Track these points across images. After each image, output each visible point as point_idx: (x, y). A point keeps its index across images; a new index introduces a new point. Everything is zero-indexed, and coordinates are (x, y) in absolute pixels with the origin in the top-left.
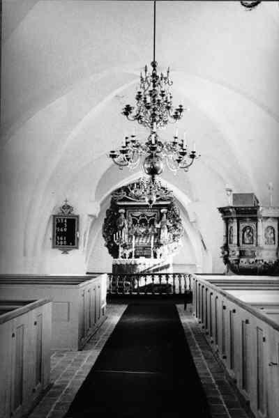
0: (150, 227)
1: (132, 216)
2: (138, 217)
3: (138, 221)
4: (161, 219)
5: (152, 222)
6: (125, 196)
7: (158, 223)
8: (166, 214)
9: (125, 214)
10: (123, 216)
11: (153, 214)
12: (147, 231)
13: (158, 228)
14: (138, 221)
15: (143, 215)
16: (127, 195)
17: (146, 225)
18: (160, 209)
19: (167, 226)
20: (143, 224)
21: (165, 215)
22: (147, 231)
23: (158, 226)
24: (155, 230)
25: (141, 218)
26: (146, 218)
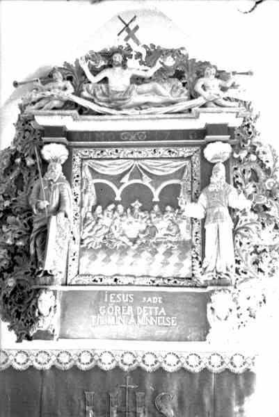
0: (163, 211)
1: (95, 174)
2: (117, 179)
3: (118, 193)
4: (206, 182)
5: (170, 199)
6: (69, 94)
7: (195, 199)
8: (226, 163)
9: (67, 167)
10: (57, 171)
11: (172, 167)
13: (193, 220)
14: (118, 193)
15: (137, 173)
16: (78, 93)
17: (147, 208)
18: (203, 146)
19: (232, 210)
20: (137, 205)
21: (222, 167)
22: (151, 231)
23: (194, 210)
24: (183, 226)
25: (126, 181)
26: (146, 181)
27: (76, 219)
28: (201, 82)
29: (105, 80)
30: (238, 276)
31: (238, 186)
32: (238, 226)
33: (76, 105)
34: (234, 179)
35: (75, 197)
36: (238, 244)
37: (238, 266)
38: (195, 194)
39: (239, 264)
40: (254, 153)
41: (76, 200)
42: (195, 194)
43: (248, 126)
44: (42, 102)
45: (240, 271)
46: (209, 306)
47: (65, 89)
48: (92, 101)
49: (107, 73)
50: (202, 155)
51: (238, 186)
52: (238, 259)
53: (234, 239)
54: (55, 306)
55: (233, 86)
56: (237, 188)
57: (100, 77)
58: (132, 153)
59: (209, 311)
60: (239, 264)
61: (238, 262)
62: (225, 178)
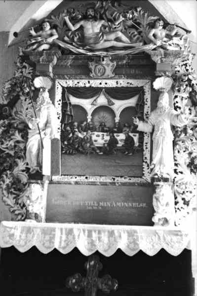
12: (113, 142)
28: (153, 31)
29: (82, 28)
30: (176, 175)
31: (178, 109)
32: (177, 139)
33: (60, 47)
34: (175, 104)
35: (58, 116)
36: (176, 152)
37: (176, 168)
38: (146, 115)
39: (177, 166)
40: (190, 86)
41: (59, 118)
42: (146, 115)
43: (186, 65)
44: (35, 47)
45: (178, 171)
46: (154, 195)
47: (51, 35)
48: (71, 44)
49: (82, 23)
50: (152, 86)
51: (178, 109)
52: (177, 162)
53: (174, 149)
54: (41, 196)
55: (176, 35)
56: (177, 110)
57: (78, 26)
58: (101, 84)
59: (154, 200)
60: (177, 166)
61: (176, 165)
62: (168, 103)
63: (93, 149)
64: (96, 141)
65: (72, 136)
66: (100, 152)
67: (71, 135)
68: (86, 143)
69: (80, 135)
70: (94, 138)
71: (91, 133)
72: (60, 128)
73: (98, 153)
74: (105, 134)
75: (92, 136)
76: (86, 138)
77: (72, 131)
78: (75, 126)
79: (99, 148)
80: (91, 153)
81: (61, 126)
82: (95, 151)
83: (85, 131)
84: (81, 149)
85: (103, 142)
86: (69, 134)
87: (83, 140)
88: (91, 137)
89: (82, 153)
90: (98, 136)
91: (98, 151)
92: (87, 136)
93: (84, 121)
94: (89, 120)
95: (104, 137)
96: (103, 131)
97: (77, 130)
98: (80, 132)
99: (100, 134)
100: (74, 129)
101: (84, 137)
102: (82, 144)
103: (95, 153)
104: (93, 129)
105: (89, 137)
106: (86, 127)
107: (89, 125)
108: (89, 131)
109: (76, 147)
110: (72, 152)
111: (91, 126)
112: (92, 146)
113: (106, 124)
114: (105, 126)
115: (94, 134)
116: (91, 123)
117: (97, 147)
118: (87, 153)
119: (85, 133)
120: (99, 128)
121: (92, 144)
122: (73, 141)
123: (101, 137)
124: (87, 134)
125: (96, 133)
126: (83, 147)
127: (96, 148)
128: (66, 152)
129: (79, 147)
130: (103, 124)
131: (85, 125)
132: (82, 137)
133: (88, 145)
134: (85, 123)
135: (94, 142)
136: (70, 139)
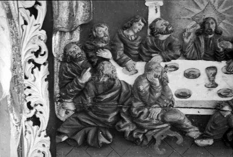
27: (38, 66)
63: (176, 126)
64: (184, 95)
65: (90, 80)
66: (201, 137)
67: (87, 76)
68: (146, 105)
69: (122, 76)
70: (176, 82)
71: (163, 64)
72: (44, 49)
73: (192, 140)
74: (221, 65)
75: (170, 75)
76: (144, 86)
77: (89, 59)
78: (98, 39)
79: (200, 121)
80: (167, 141)
81: (49, 43)
82: (183, 132)
83: (139, 59)
84: (128, 128)
85: (213, 96)
86: (80, 73)
87: (134, 91)
88: (164, 82)
89: (133, 142)
90: (190, 75)
91: (194, 133)
92: (151, 76)
93: (134, 20)
94: (153, 15)
95: (218, 80)
96: (216, 56)
97: (107, 54)
98: (121, 64)
99: (201, 65)
100: (96, 49)
101: (138, 82)
102: (130, 106)
103: (180, 140)
104: (171, 50)
105: (157, 82)
106: (144, 43)
107: (154, 32)
108: (157, 58)
109: (111, 119)
110: (96, 135)
111: (163, 37)
112: (171, 117)
113: (221, 26)
114: (218, 33)
115: (176, 68)
116: (160, 25)
117: (190, 117)
118: (154, 140)
119: (140, 66)
120: (196, 43)
121: (169, 108)
122: (96, 97)
123: (203, 79)
124: (148, 69)
125: (184, 65)
126: (134, 119)
127: (187, 123)
128: (71, 142)
129: (119, 118)
130: (213, 27)
131: (137, 34)
132: (130, 80)
133: (157, 111)
134: (139, 26)
135: (176, 99)
136: (83, 91)
